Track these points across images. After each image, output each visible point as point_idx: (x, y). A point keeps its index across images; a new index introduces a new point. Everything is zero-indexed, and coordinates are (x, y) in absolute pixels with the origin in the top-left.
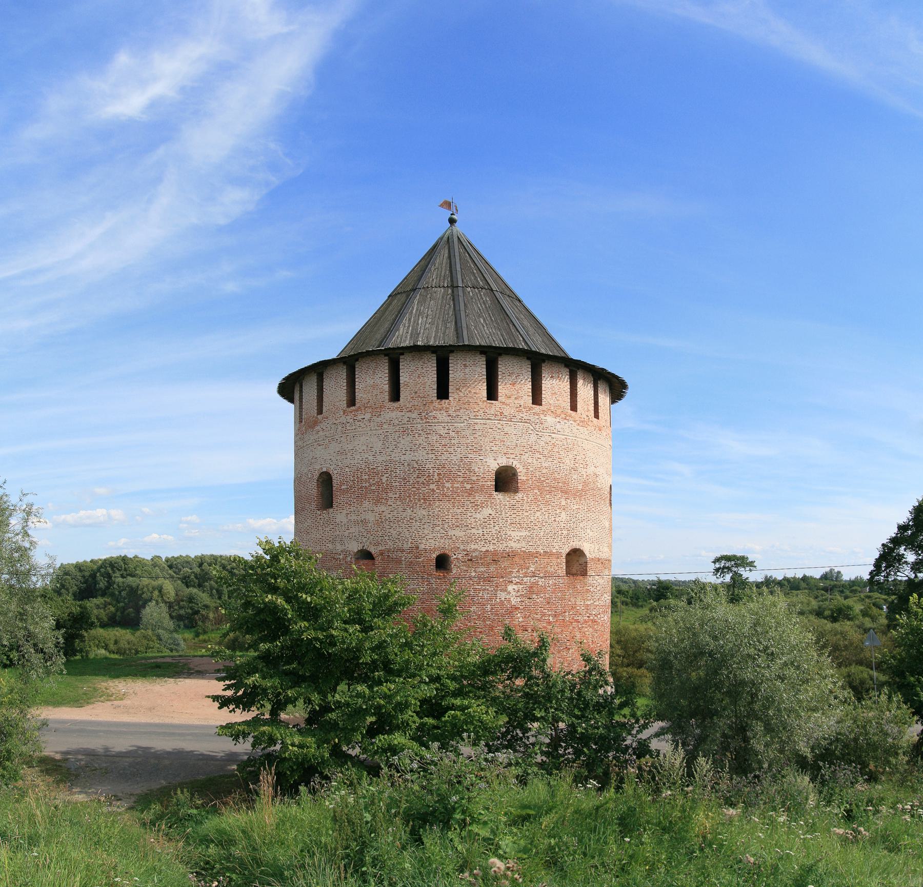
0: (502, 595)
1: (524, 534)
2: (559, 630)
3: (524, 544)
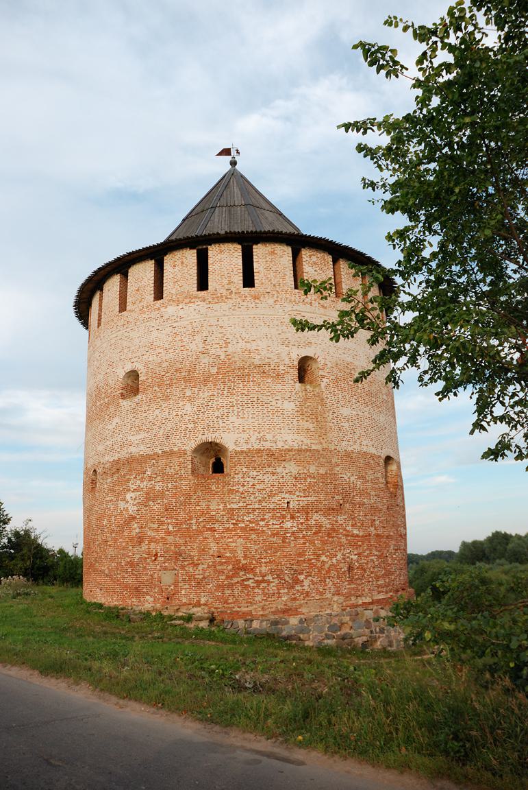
0: (122, 505)
1: (142, 436)
2: (182, 541)
3: (142, 447)
